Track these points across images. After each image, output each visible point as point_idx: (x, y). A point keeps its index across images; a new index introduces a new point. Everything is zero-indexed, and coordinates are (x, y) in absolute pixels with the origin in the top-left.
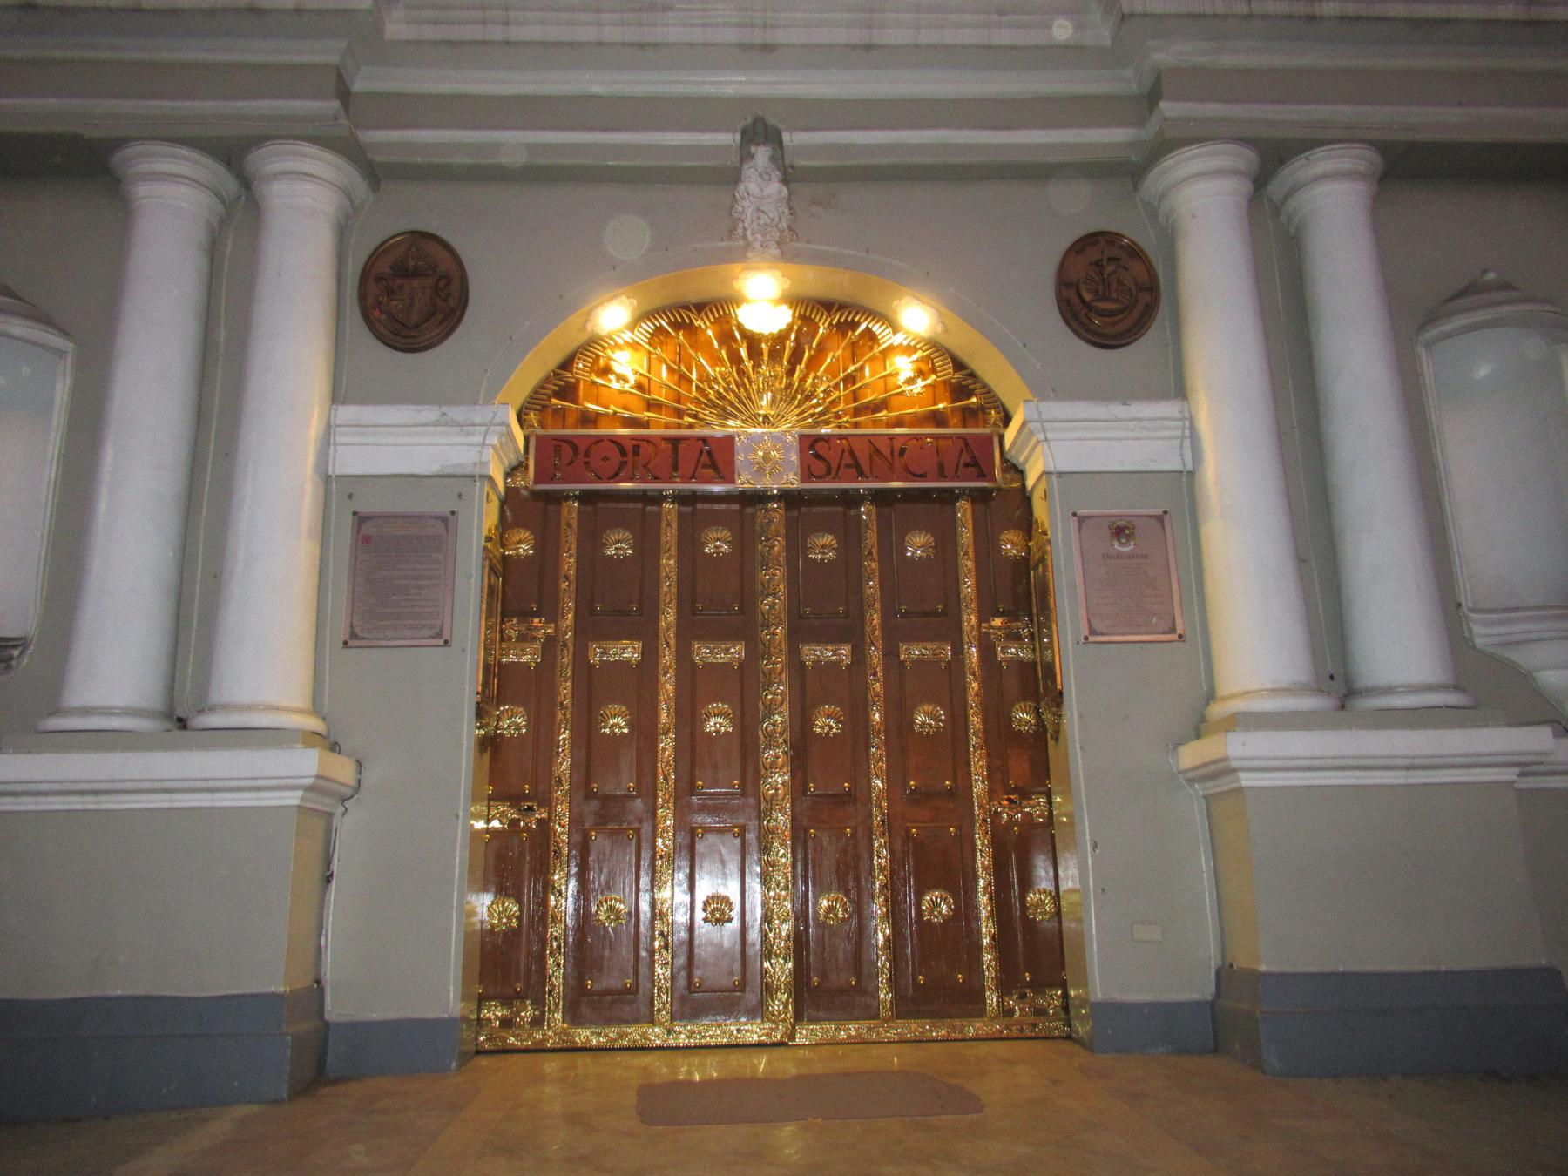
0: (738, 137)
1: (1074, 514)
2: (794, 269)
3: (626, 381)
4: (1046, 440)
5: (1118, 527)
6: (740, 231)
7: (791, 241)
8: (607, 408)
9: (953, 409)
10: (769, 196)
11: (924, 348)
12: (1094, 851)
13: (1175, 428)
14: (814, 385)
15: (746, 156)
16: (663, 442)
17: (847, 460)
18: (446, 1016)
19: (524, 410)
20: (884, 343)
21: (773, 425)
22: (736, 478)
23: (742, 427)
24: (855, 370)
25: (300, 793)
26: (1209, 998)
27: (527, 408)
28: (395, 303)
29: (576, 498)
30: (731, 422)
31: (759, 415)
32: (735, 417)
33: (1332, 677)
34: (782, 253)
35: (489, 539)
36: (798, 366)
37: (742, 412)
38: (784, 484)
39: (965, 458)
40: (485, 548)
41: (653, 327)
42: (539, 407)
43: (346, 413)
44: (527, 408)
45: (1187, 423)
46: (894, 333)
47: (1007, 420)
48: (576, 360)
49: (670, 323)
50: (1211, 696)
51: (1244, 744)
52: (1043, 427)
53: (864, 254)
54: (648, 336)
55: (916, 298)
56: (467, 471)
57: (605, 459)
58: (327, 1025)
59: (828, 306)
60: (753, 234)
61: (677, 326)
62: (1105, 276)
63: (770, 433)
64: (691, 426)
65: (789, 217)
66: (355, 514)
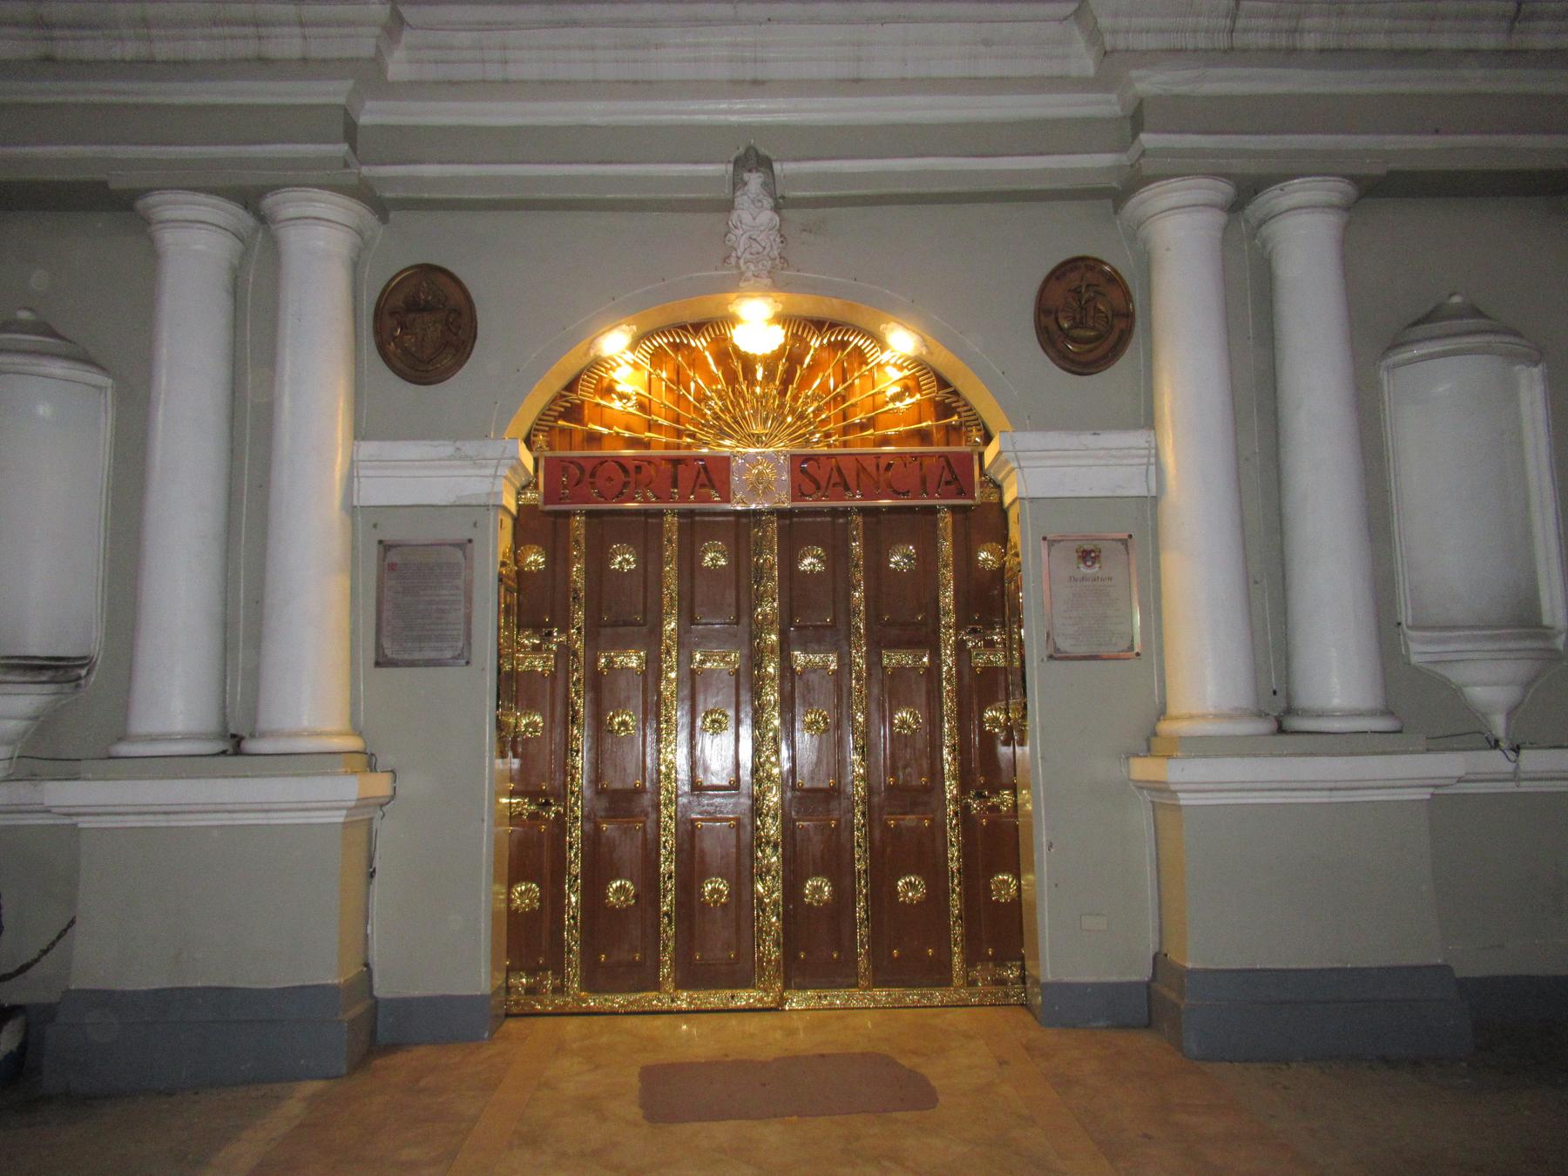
0: (730, 167)
1: (1044, 539)
2: (783, 296)
3: (629, 399)
4: (1020, 467)
5: (1084, 551)
6: (733, 260)
7: (782, 269)
8: (610, 428)
9: (937, 426)
10: (762, 225)
11: (910, 367)
12: (1049, 850)
13: (1142, 457)
14: (805, 404)
15: (738, 184)
16: (663, 462)
17: (836, 478)
18: (479, 993)
19: (533, 432)
20: (873, 361)
21: (766, 444)
22: (732, 497)
23: (737, 447)
24: (845, 389)
25: (344, 812)
26: (1146, 979)
27: (535, 430)
28: (409, 337)
29: (580, 514)
30: (727, 442)
31: (753, 435)
32: (731, 437)
33: (1275, 693)
34: (773, 281)
35: (503, 564)
36: (790, 386)
37: (737, 432)
38: (776, 503)
39: (946, 476)
40: (500, 574)
41: (653, 348)
42: (547, 429)
43: (369, 448)
44: (535, 430)
45: (1153, 451)
46: (882, 352)
47: (988, 439)
48: (581, 382)
49: (669, 344)
50: (1162, 713)
51: (1183, 770)
52: (1016, 456)
53: (853, 282)
54: (649, 356)
55: (901, 324)
56: (482, 502)
57: (610, 479)
58: (376, 1000)
59: (819, 325)
60: (745, 263)
61: (676, 347)
62: (1083, 302)
63: (764, 453)
64: (689, 446)
65: (781, 245)
66: (380, 542)
